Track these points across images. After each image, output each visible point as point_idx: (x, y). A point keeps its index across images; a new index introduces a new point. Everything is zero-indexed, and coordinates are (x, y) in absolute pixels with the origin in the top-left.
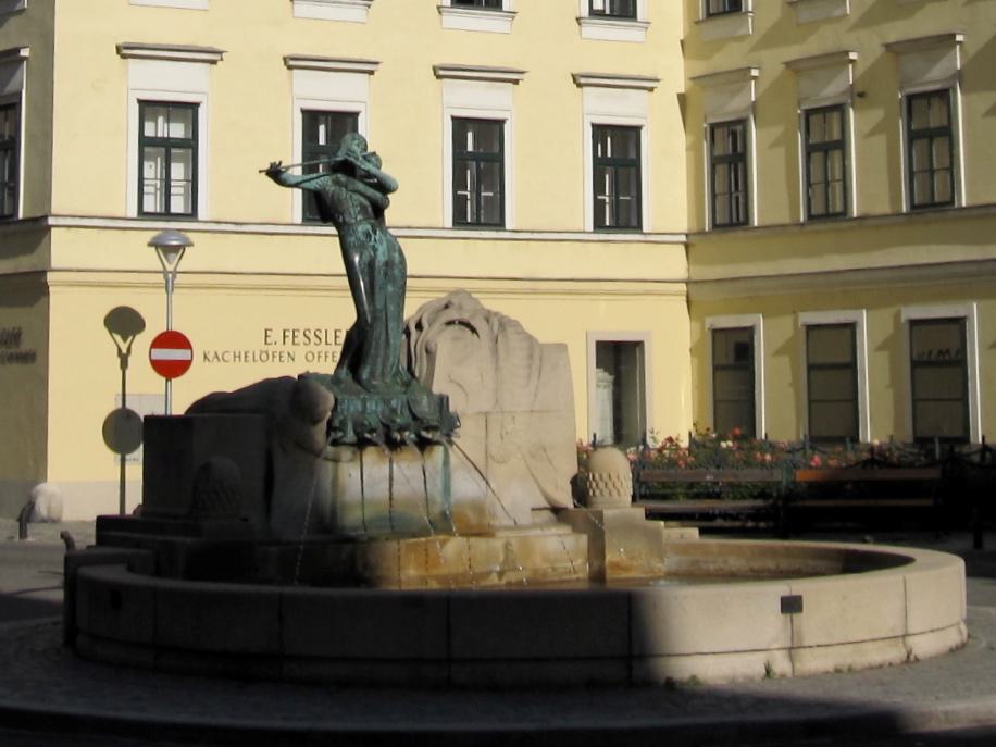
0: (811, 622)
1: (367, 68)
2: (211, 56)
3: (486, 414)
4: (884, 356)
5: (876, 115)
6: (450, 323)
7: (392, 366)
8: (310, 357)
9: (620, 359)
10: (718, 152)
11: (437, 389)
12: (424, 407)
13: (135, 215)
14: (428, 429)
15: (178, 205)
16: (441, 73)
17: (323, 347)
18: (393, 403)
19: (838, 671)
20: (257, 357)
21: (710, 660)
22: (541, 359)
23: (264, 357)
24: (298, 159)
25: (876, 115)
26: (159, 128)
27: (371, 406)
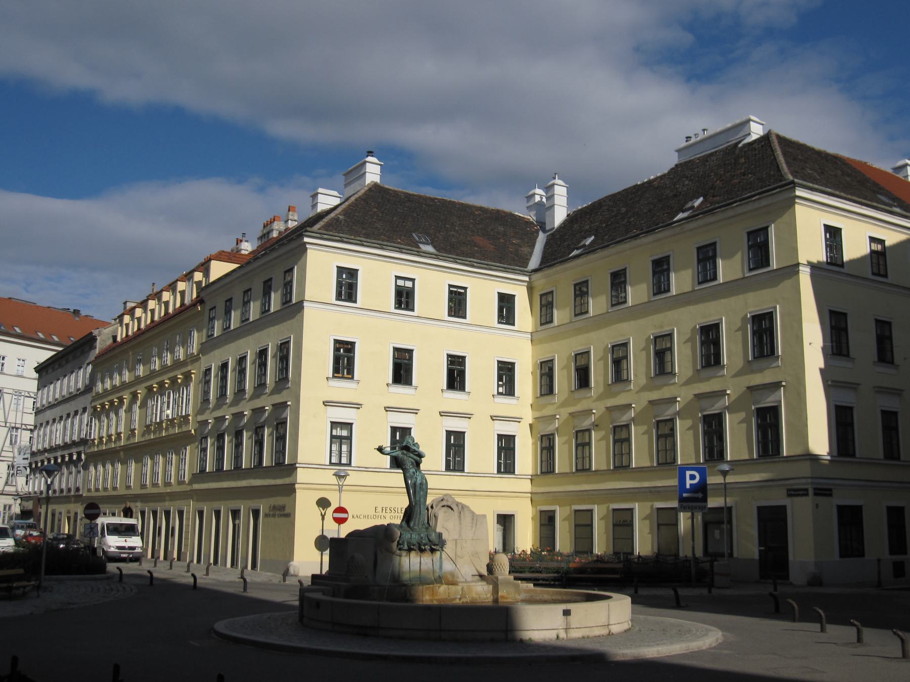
0: (574, 619)
1: (415, 412)
2: (358, 406)
4: (603, 522)
5: (602, 433)
9: (506, 521)
10: (544, 445)
11: (438, 531)
12: (433, 537)
13: (328, 463)
14: (435, 545)
15: (344, 461)
16: (442, 414)
17: (396, 514)
19: (583, 637)
21: (536, 632)
24: (389, 445)
25: (602, 433)
26: (338, 432)
27: (414, 536)
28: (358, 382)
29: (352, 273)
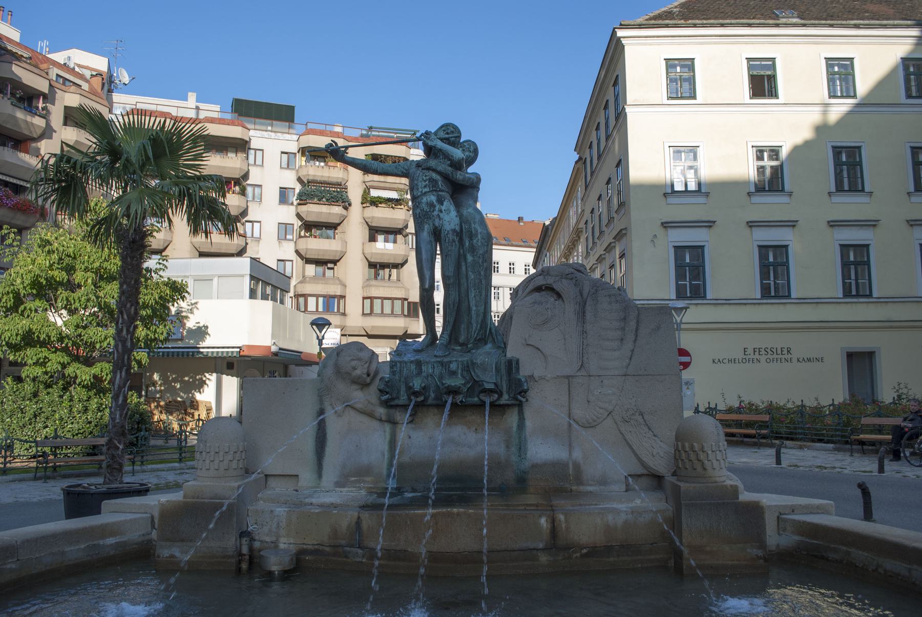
2: (710, 224)
3: (568, 377)
6: (539, 289)
11: (509, 354)
17: (775, 356)
18: (453, 366)
22: (638, 322)
29: (689, 64)
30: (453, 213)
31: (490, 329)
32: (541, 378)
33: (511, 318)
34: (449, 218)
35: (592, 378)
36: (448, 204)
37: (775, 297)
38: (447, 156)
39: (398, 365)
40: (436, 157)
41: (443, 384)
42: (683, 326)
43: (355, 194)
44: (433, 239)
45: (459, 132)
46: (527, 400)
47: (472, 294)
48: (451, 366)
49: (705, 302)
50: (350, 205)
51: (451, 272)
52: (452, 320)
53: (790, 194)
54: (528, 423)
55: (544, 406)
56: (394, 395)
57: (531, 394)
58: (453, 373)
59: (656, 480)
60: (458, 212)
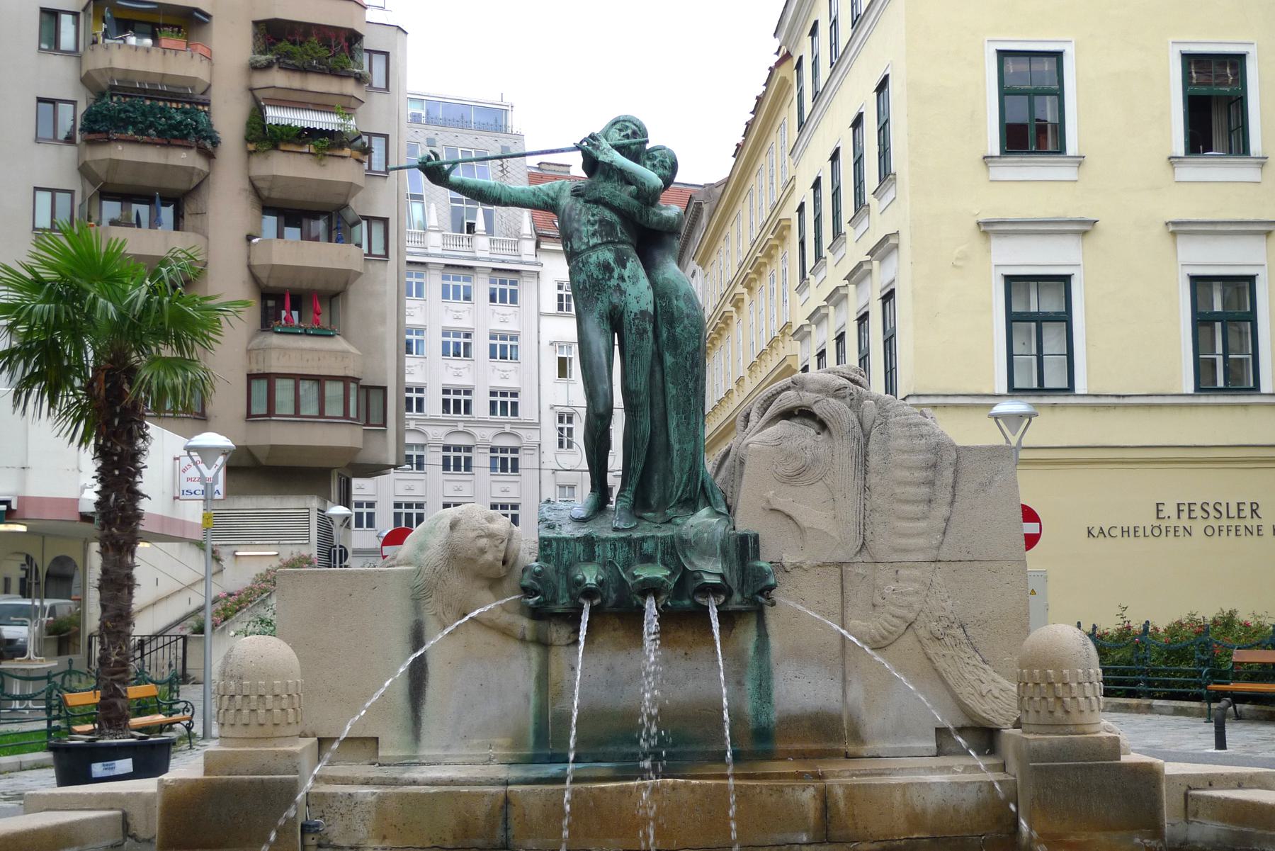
2: (1084, 228)
3: (840, 564)
6: (787, 415)
7: (678, 488)
8: (1209, 531)
17: (1224, 522)
18: (648, 547)
20: (1148, 532)
22: (956, 471)
23: (1156, 532)
28: (1079, 160)
30: (644, 282)
31: (703, 483)
32: (795, 566)
33: (742, 463)
34: (638, 292)
35: (879, 565)
36: (634, 266)
37: (1225, 391)
38: (625, 177)
39: (554, 544)
40: (608, 177)
41: (635, 577)
42: (1023, 455)
43: (228, 118)
44: (608, 328)
45: (645, 134)
46: (773, 604)
47: (672, 424)
48: (645, 545)
49: (1071, 400)
50: (216, 142)
51: (641, 382)
52: (640, 466)
53: (1262, 162)
54: (774, 643)
55: (798, 610)
56: (549, 597)
57: (777, 595)
58: (648, 559)
59: (985, 737)
60: (649, 275)
